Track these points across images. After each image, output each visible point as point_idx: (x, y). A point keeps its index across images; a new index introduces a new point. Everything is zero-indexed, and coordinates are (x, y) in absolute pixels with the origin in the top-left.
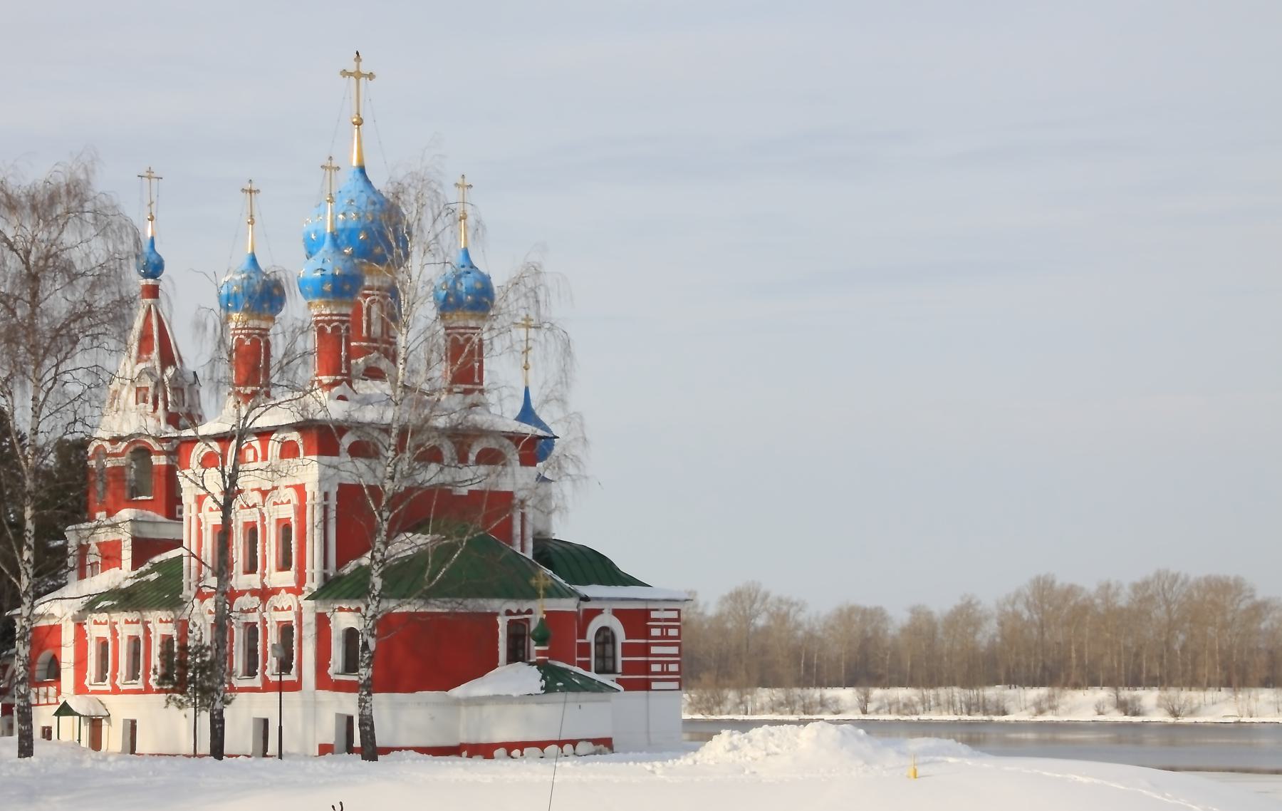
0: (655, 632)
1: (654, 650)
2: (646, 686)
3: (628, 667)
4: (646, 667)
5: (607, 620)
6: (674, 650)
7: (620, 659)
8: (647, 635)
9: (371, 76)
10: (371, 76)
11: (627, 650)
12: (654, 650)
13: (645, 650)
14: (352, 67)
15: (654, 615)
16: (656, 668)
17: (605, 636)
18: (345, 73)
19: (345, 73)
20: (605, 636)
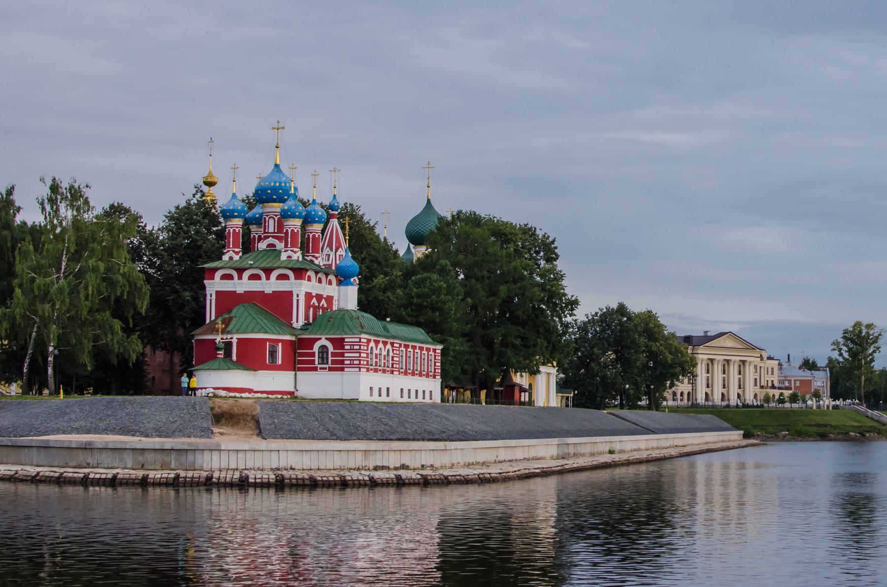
0: (346, 347)
1: (346, 355)
2: (342, 369)
3: (333, 362)
4: (342, 362)
5: (324, 342)
6: (358, 355)
7: (330, 358)
8: (343, 348)
9: (283, 128)
10: (283, 128)
11: (333, 354)
12: (346, 355)
13: (342, 355)
14: (276, 126)
15: (346, 340)
16: (346, 362)
17: (324, 348)
18: (273, 128)
19: (273, 128)
20: (324, 348)
